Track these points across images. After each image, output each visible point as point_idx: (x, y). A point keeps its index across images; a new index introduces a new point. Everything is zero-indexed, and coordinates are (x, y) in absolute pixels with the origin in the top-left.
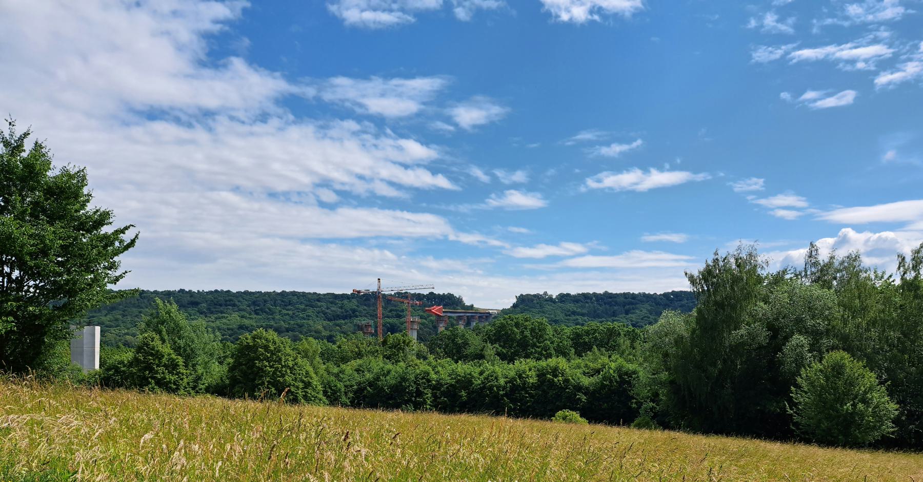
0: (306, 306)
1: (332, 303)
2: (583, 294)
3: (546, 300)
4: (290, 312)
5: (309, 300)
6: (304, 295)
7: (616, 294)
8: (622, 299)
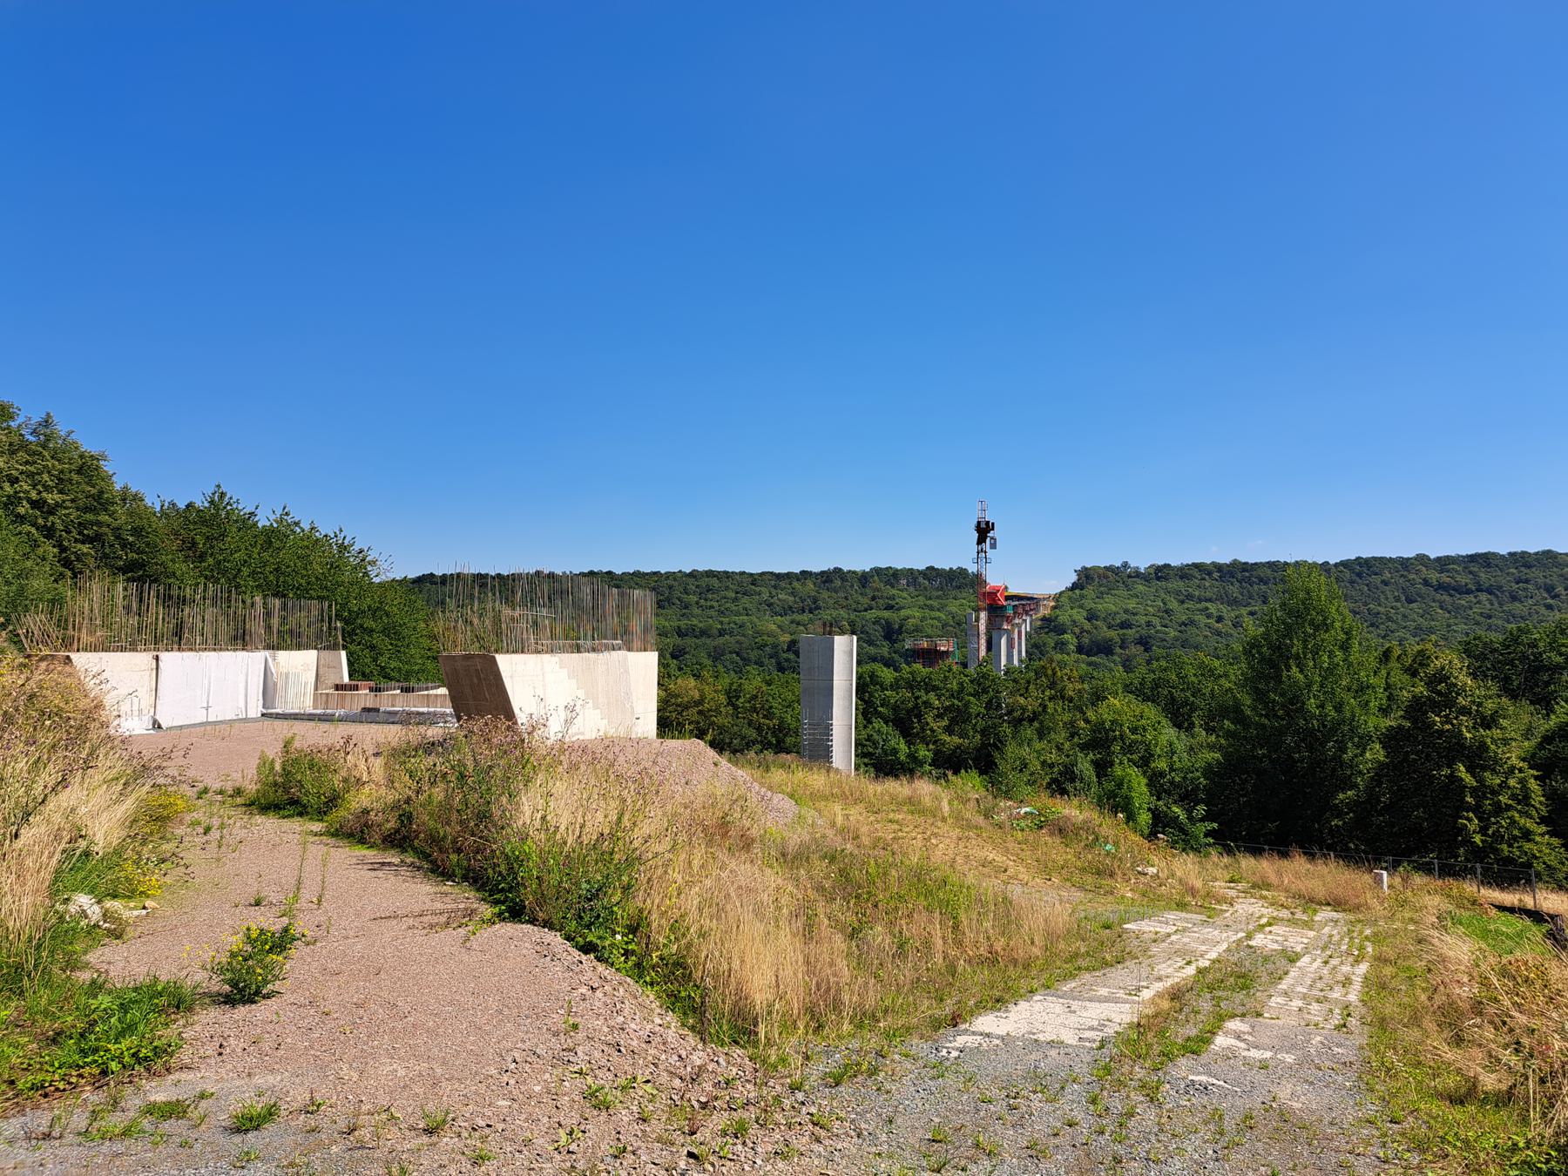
0: (737, 593)
1: (775, 587)
2: (1196, 566)
3: (1129, 576)
4: (715, 604)
5: (740, 584)
6: (727, 575)
7: (1256, 564)
8: (1269, 572)
